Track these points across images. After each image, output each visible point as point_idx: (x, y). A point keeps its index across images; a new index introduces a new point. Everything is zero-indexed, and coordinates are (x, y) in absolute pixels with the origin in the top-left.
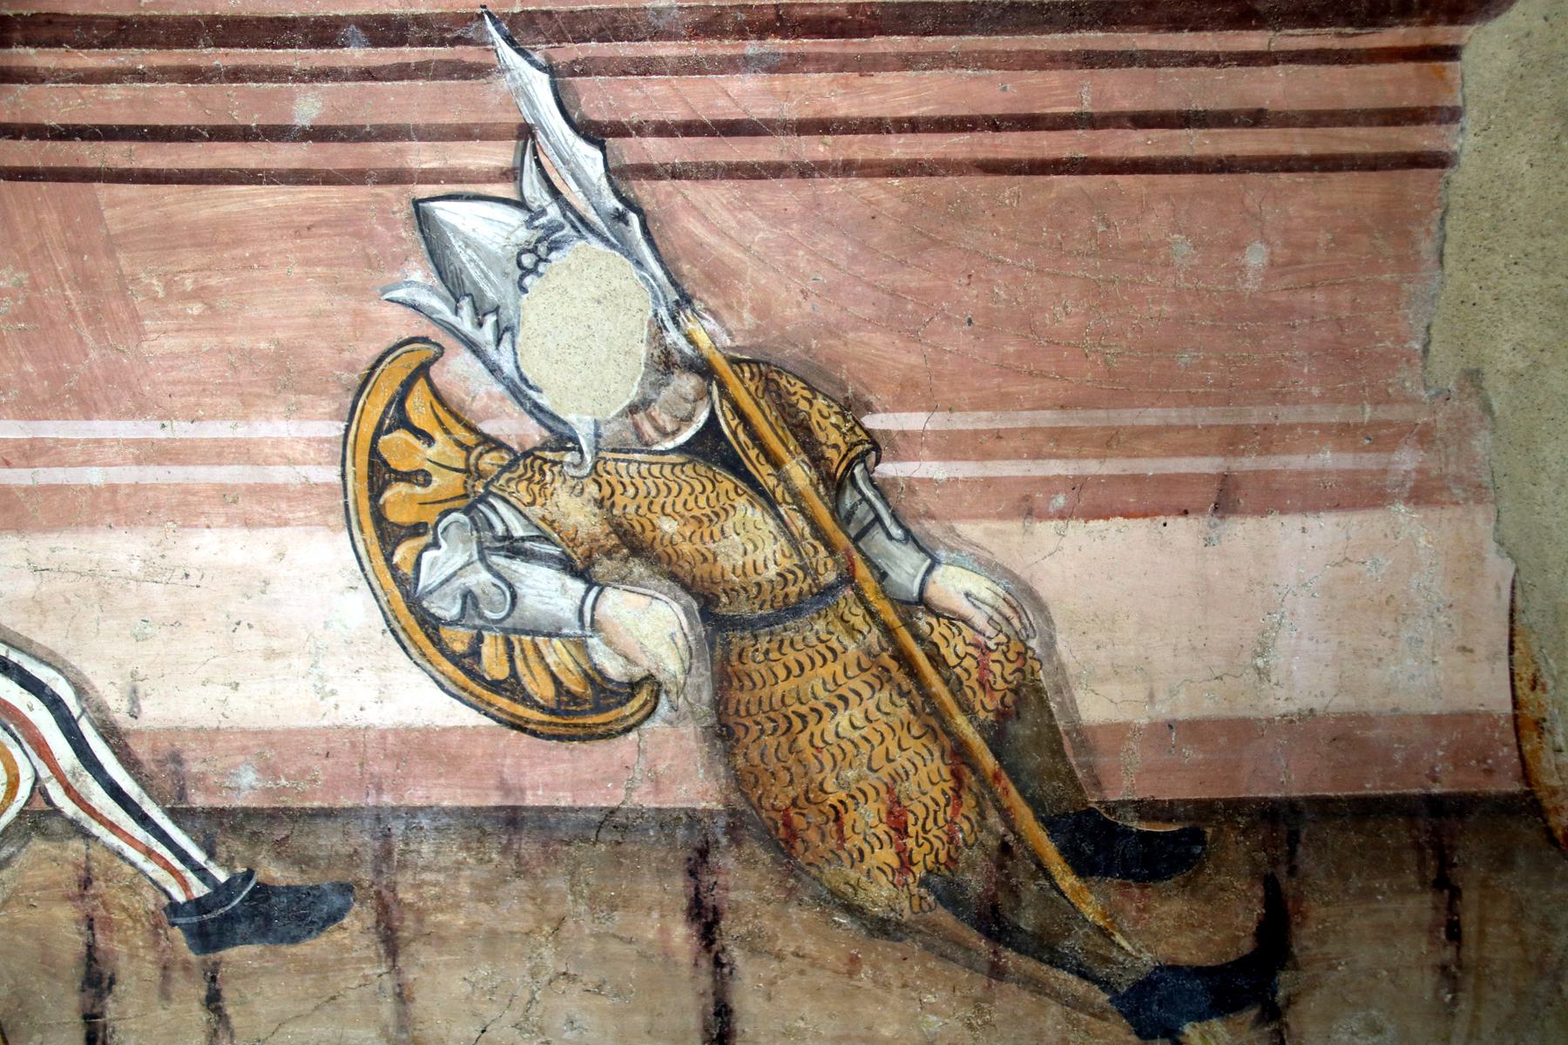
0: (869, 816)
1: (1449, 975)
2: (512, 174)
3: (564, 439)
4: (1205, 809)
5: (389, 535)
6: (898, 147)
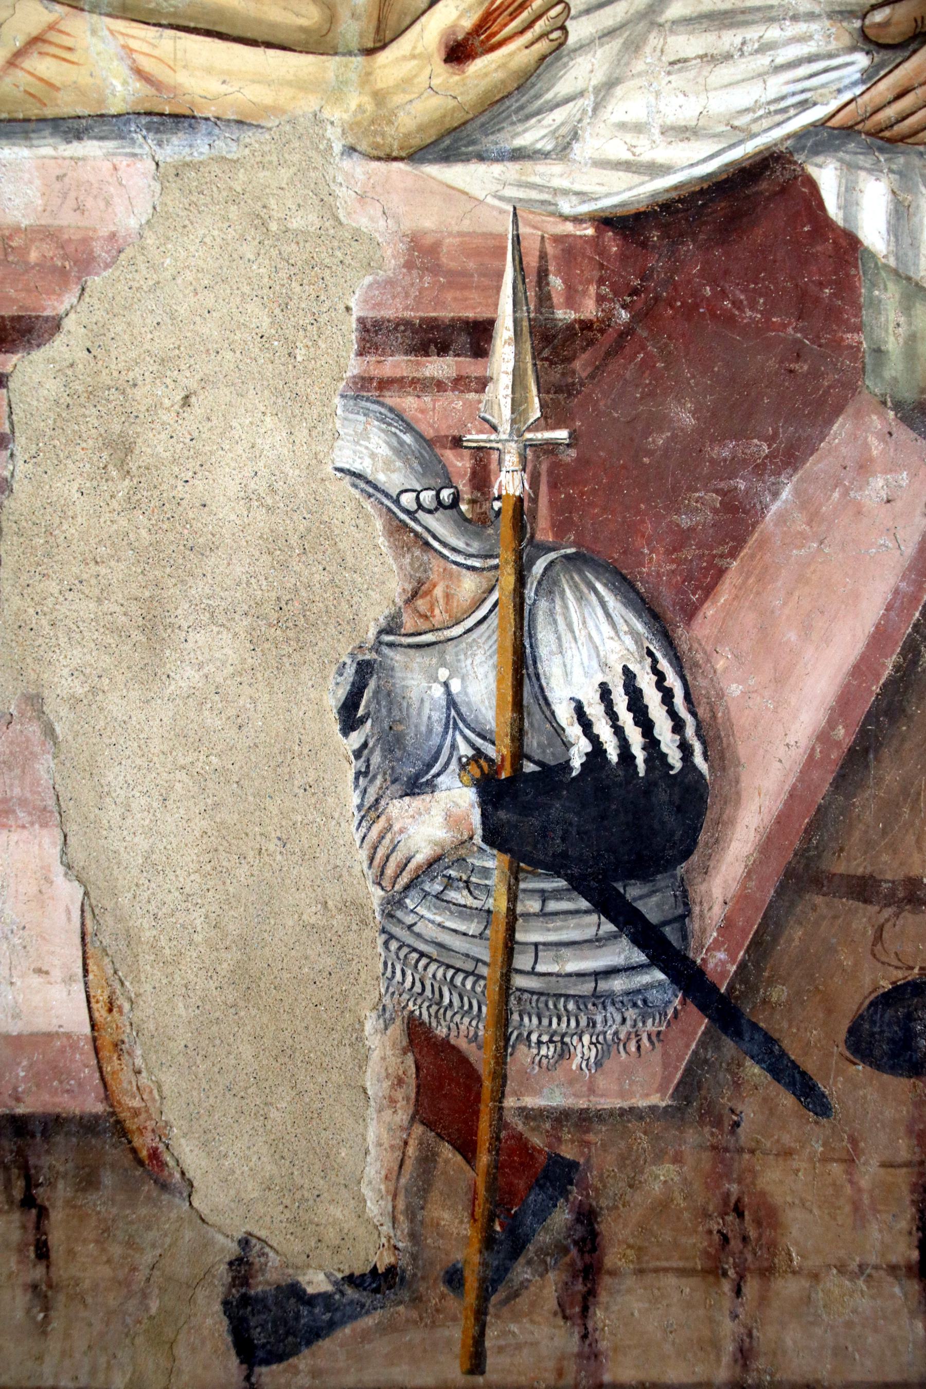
1: (42, 1295)
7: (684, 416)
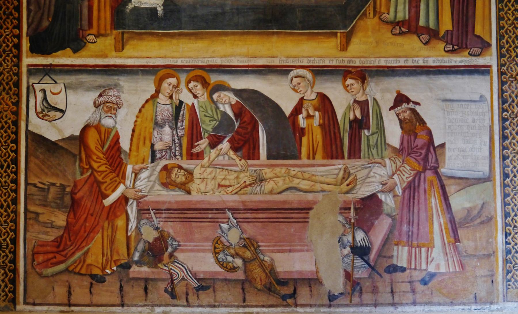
0: (258, 280)
1: (311, 295)
2: (228, 222)
3: (232, 245)
4: (289, 279)
5: (216, 253)
6: (262, 220)
7: (368, 215)
